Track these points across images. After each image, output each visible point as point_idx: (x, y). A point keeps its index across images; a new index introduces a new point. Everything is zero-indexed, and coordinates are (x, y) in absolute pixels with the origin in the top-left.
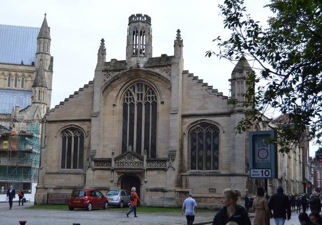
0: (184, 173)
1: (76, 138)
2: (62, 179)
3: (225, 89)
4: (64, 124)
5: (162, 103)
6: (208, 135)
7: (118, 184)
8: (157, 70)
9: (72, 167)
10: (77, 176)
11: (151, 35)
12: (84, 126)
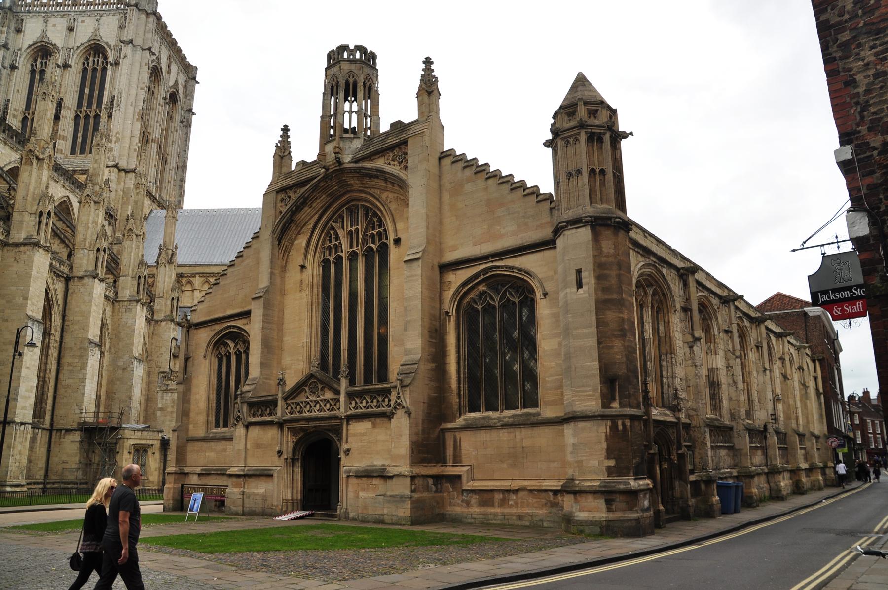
0: (450, 422)
3: (538, 170)
4: (218, 327)
5: (397, 241)
7: (293, 460)
11: (377, 91)
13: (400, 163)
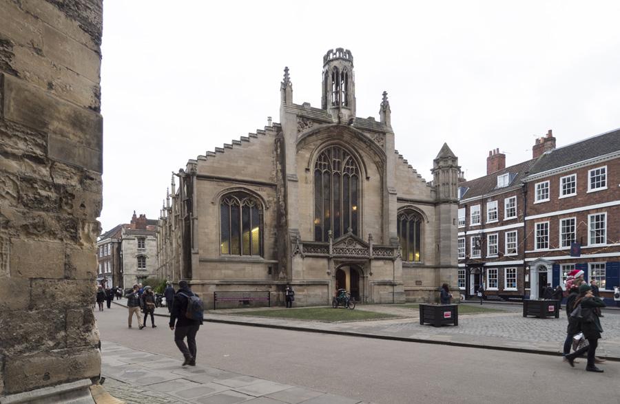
1: (246, 208)
4: (227, 185)
5: (368, 178)
6: (412, 222)
8: (368, 135)
10: (256, 266)
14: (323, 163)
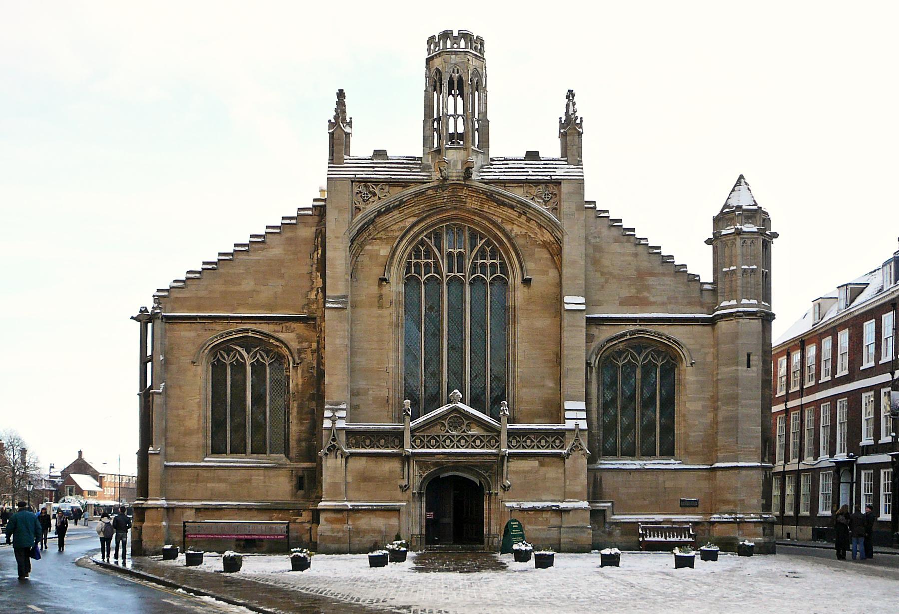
1: (258, 369)
2: (220, 480)
4: (219, 327)
5: (527, 282)
6: (648, 369)
7: (420, 494)
9: (249, 449)
12: (289, 336)
13: (546, 202)
14: (423, 261)
